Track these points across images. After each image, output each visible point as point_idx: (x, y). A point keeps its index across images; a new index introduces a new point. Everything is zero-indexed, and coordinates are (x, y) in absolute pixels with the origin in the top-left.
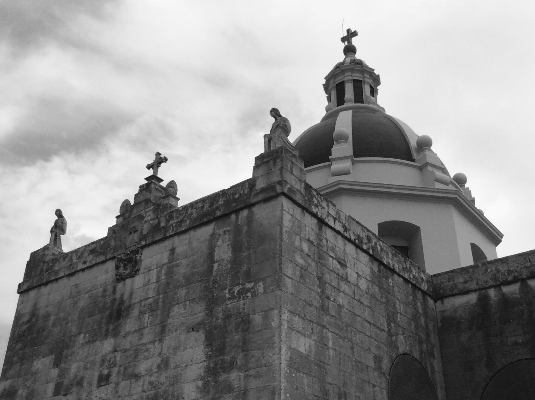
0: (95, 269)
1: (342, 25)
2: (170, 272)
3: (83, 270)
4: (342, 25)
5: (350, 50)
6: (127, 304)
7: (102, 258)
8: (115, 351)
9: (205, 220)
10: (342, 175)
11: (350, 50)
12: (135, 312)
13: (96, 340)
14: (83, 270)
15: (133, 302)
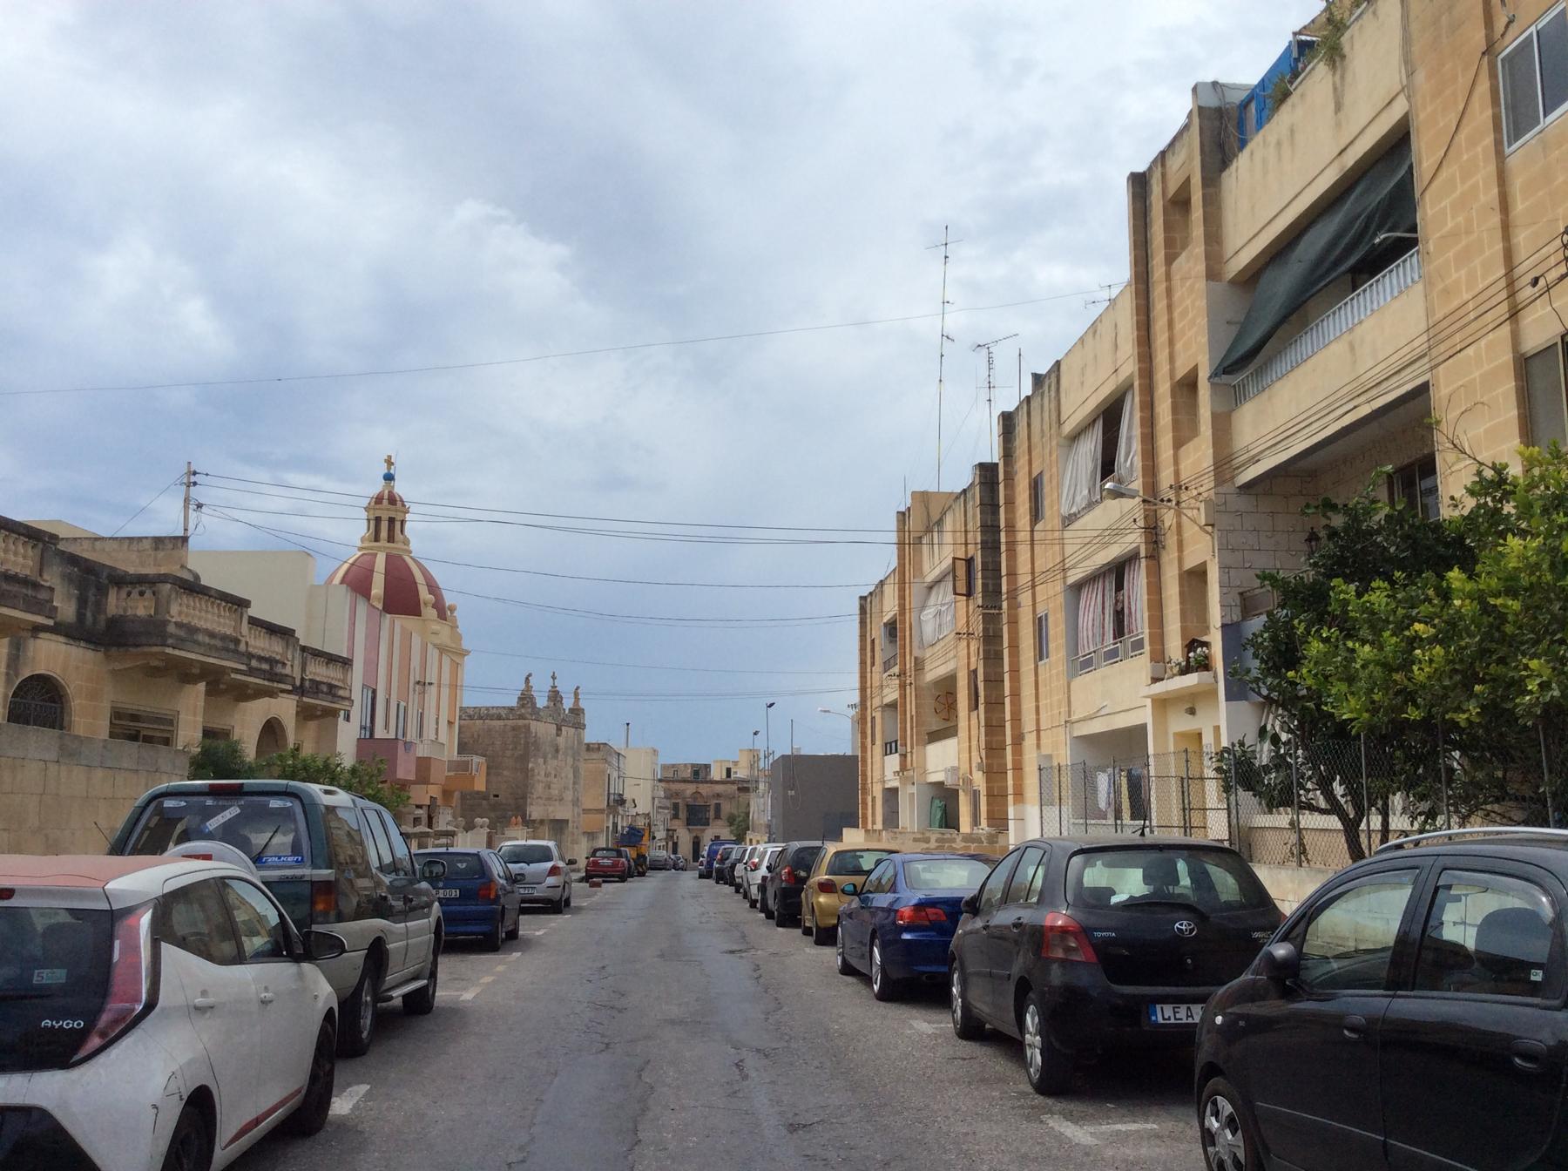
5: (389, 478)
11: (389, 478)
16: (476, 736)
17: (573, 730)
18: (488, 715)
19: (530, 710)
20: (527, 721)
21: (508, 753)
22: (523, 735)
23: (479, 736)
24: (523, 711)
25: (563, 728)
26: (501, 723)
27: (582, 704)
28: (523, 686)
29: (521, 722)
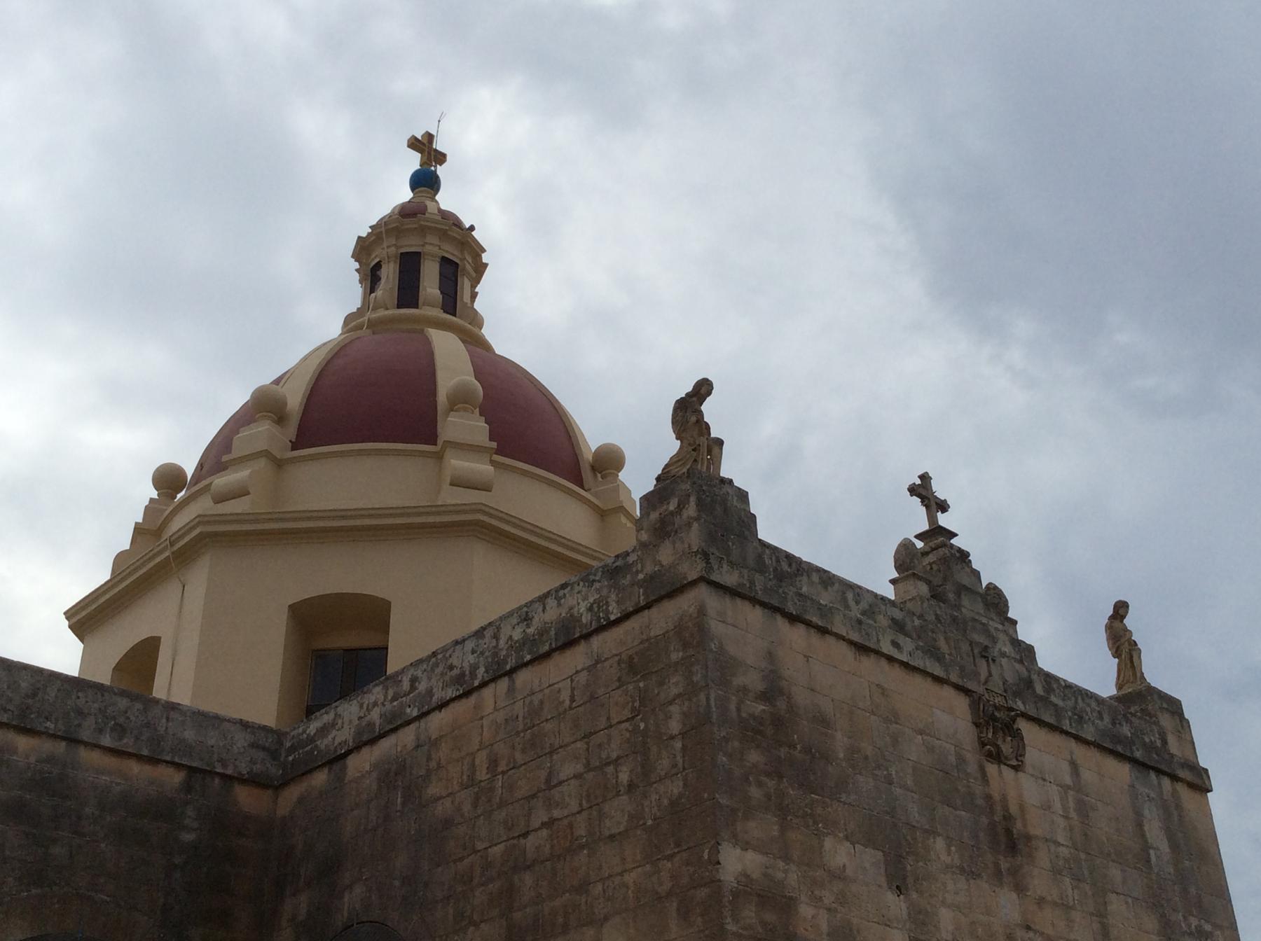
0: (918, 679)
1: (439, 121)
2: (1084, 810)
3: (890, 659)
4: (439, 121)
5: (425, 181)
6: (1019, 825)
7: (938, 671)
8: (1028, 928)
9: (1120, 749)
10: (473, 489)
11: (425, 181)
12: (1043, 857)
13: (979, 876)
14: (890, 659)
15: (1033, 831)
16: (482, 775)
17: (1123, 771)
18: (526, 641)
19: (694, 537)
20: (685, 603)
21: (617, 814)
22: (675, 685)
23: (493, 763)
24: (666, 555)
25: (1022, 725)
26: (576, 658)
27: (1157, 673)
28: (672, 446)
29: (662, 619)
